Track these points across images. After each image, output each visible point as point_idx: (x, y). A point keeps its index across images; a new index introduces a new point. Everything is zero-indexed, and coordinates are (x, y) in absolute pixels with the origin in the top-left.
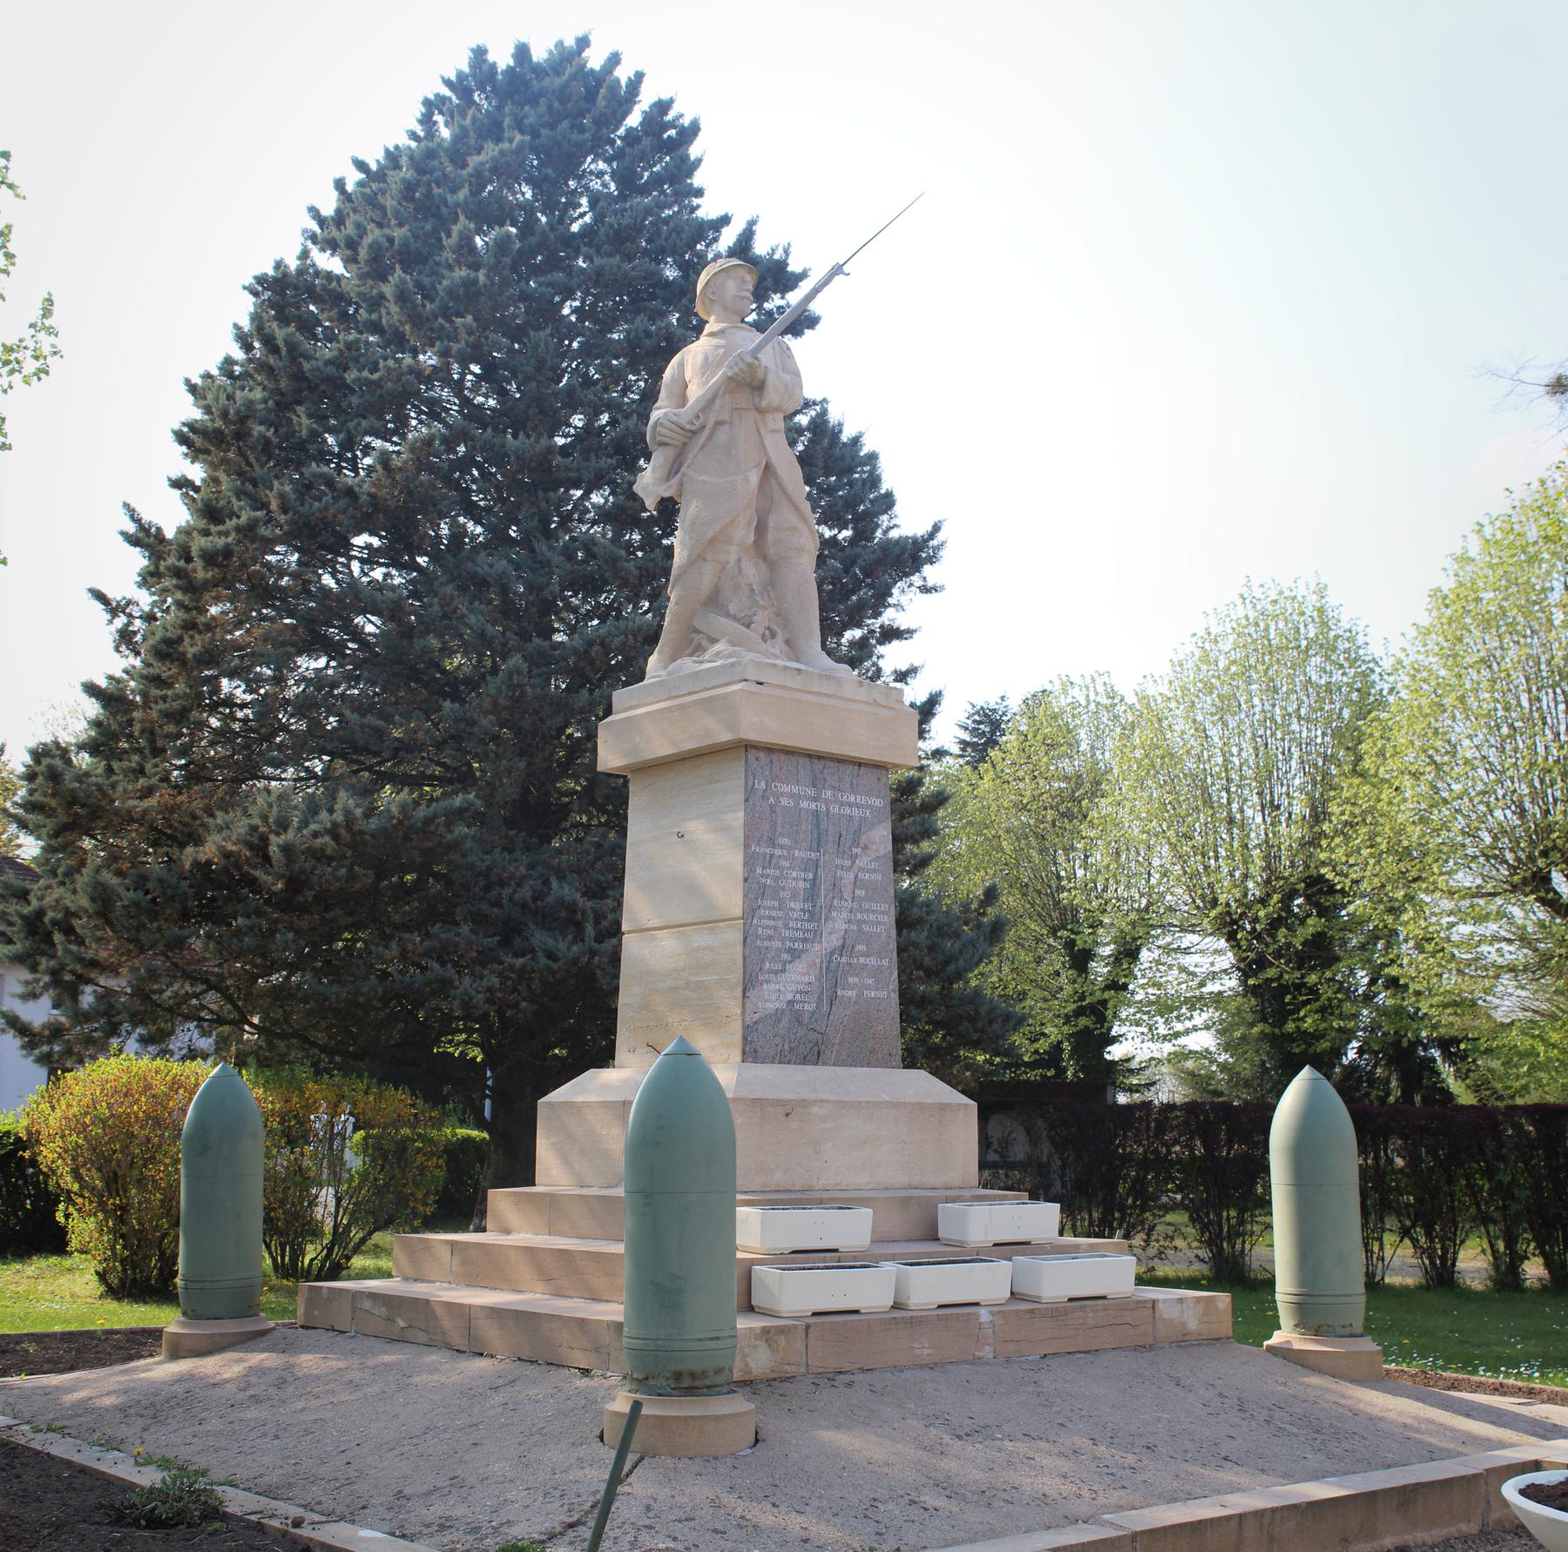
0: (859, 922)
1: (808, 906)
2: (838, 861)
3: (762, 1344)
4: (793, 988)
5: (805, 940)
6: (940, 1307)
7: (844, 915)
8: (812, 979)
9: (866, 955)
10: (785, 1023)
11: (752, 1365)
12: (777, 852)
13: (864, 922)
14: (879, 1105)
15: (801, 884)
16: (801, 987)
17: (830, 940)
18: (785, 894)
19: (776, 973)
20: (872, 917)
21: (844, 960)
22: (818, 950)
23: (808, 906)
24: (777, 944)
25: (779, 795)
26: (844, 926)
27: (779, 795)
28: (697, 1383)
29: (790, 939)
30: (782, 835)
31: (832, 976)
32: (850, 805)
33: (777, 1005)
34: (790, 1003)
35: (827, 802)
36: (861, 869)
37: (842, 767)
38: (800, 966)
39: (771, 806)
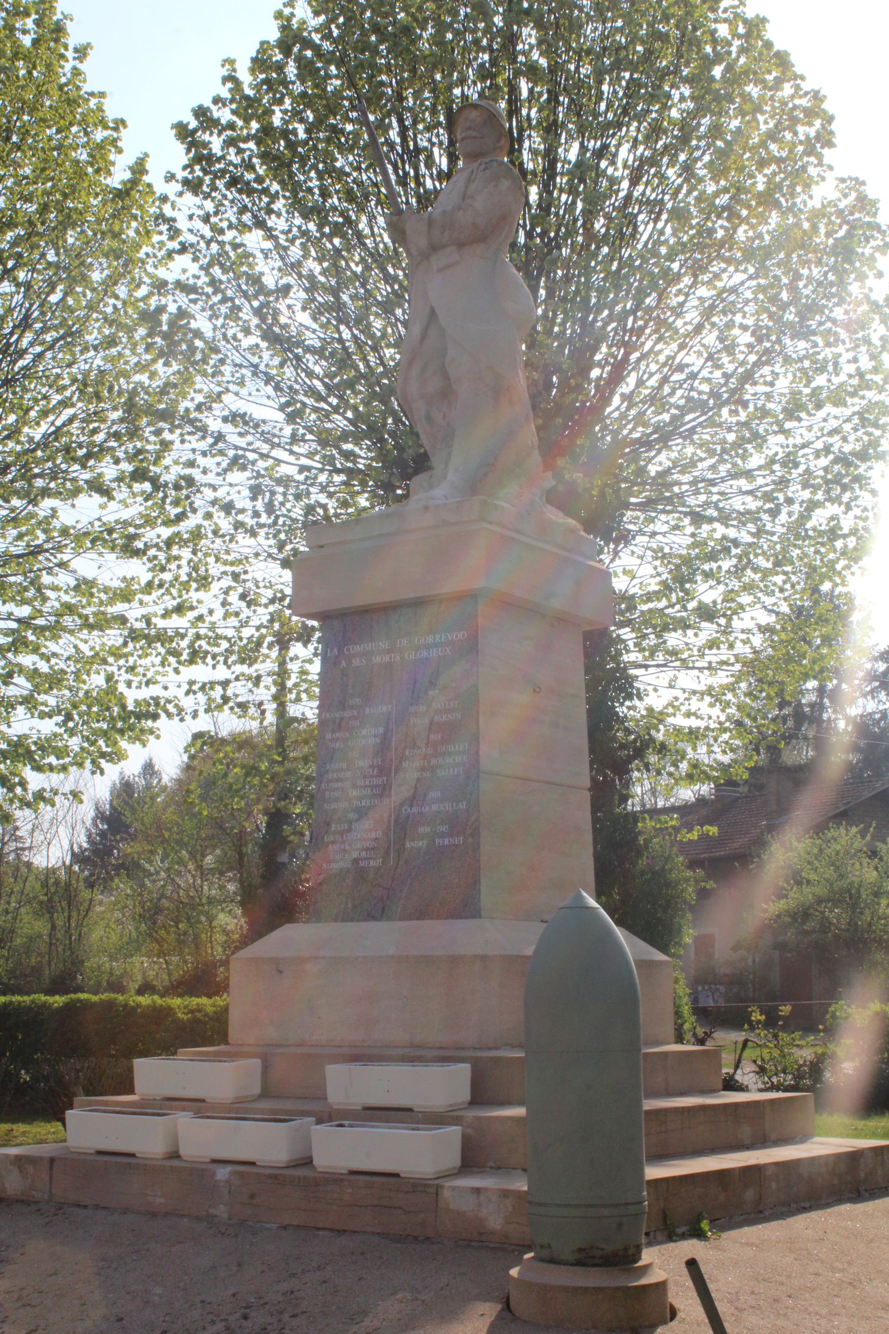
4: (359, 846)
8: (379, 834)
11: (7, 1185)
12: (347, 714)
15: (371, 741)
16: (367, 844)
17: (400, 792)
26: (416, 775)
34: (356, 861)
38: (367, 823)
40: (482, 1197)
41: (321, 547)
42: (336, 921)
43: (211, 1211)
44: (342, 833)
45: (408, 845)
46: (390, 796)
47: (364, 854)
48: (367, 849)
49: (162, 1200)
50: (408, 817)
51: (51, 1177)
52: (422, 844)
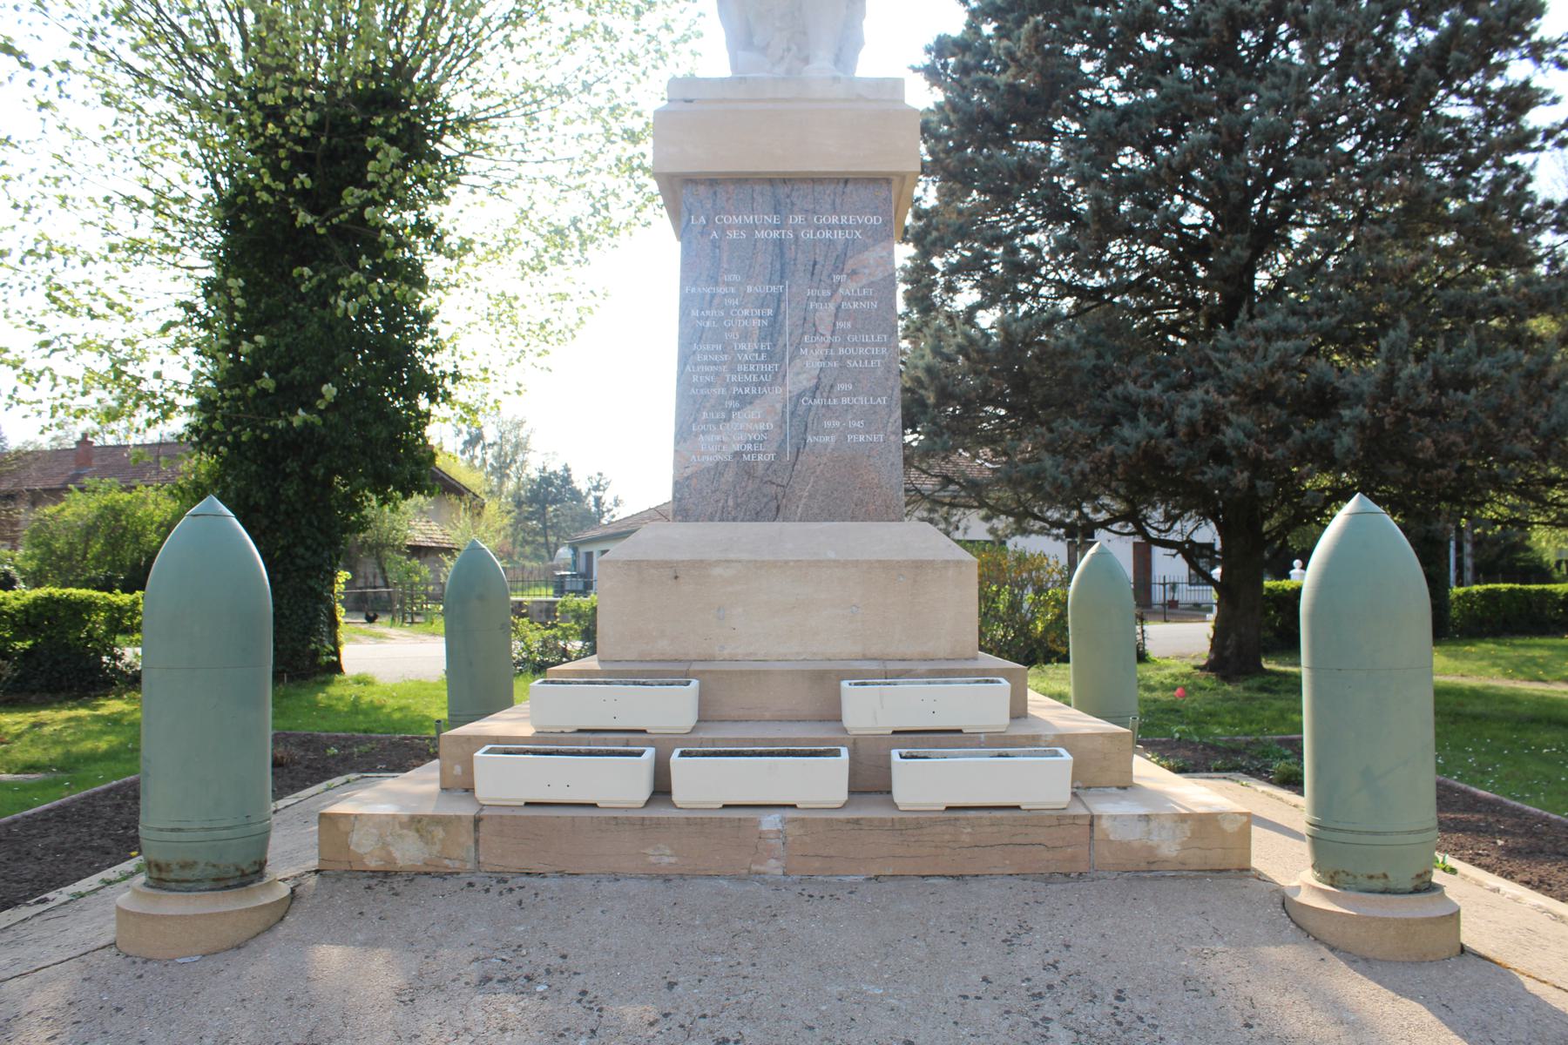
0: (841, 359)
3: (411, 835)
7: (820, 352)
8: (770, 426)
10: (729, 476)
11: (397, 854)
12: (721, 290)
13: (849, 357)
14: (818, 564)
15: (756, 323)
17: (799, 378)
21: (817, 402)
22: (778, 395)
25: (723, 229)
26: (818, 364)
27: (723, 229)
28: (164, 876)
29: (738, 384)
30: (729, 271)
31: (799, 420)
32: (830, 227)
33: (719, 457)
34: (737, 454)
35: (795, 230)
36: (849, 298)
37: (819, 188)
38: (753, 413)
39: (713, 242)
40: (1153, 824)
42: (711, 519)
43: (754, 868)
44: (717, 423)
45: (810, 439)
46: (783, 384)
48: (753, 442)
49: (673, 860)
50: (809, 409)
51: (477, 842)
52: (831, 440)
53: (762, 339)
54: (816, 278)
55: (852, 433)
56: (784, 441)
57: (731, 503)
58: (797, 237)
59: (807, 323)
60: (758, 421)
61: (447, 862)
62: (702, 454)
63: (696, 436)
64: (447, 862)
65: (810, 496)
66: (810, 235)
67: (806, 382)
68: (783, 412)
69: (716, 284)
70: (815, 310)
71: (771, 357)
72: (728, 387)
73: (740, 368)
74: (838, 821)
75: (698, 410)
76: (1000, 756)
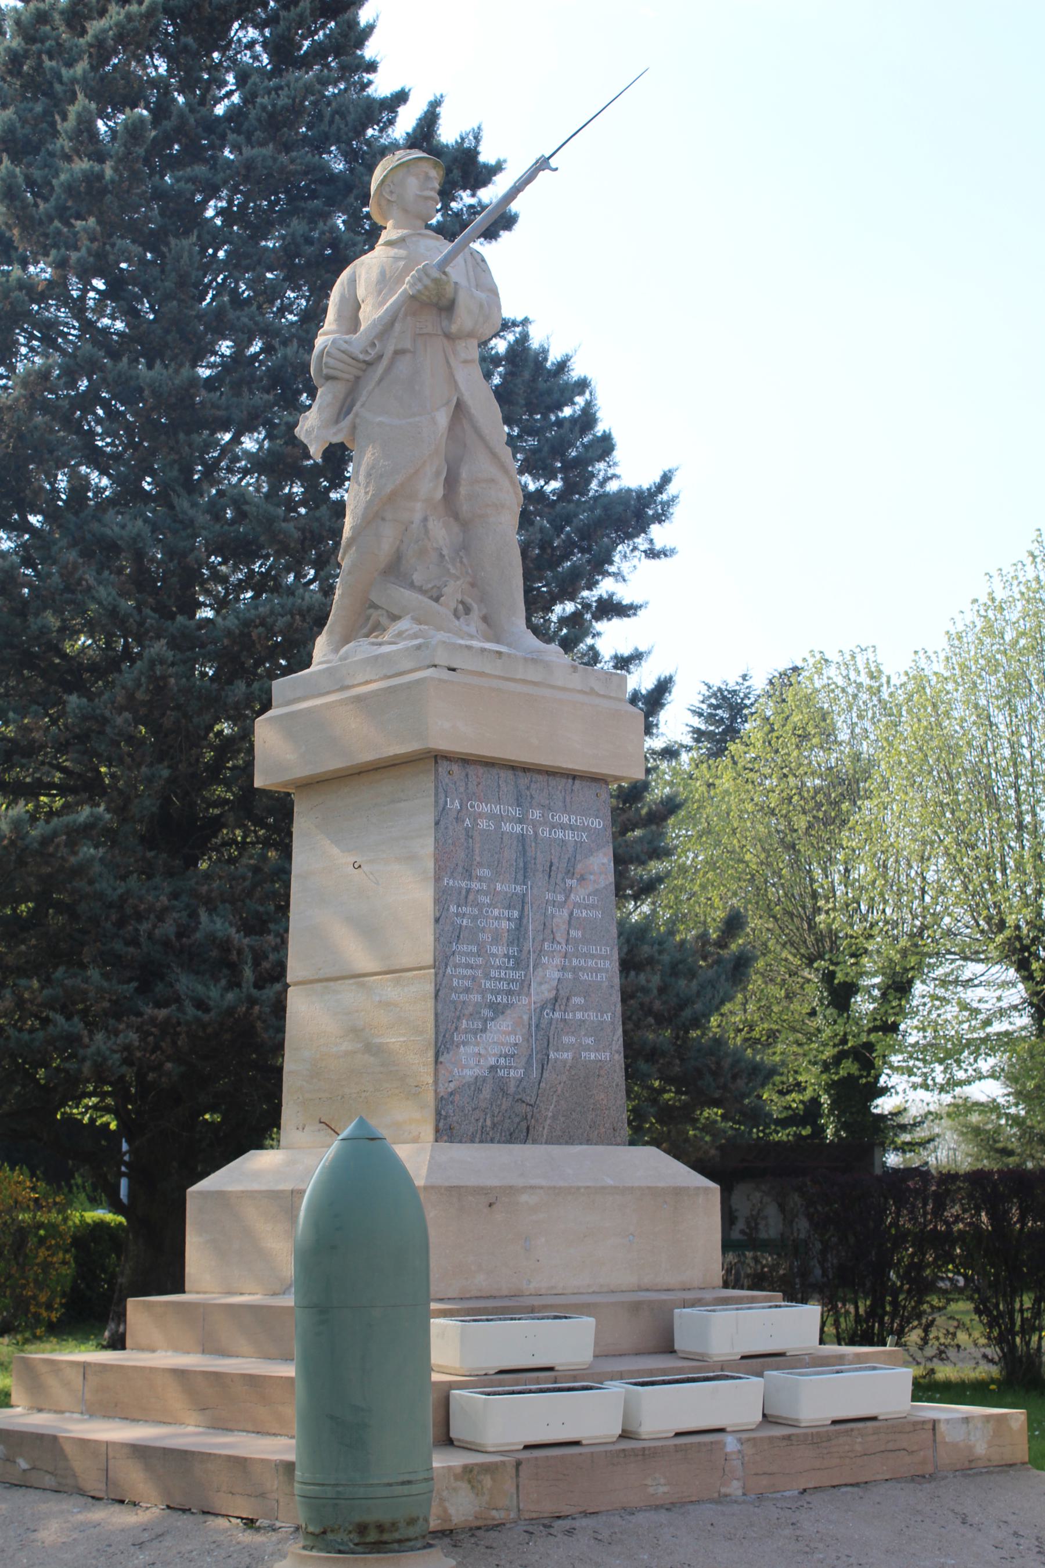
0: (575, 970)
1: (513, 950)
2: (549, 896)
3: (464, 1486)
4: (496, 1051)
5: (509, 993)
6: (678, 1434)
7: (558, 961)
8: (519, 1039)
9: (584, 1008)
10: (486, 1093)
11: (452, 1511)
12: (475, 885)
13: (581, 969)
14: (603, 1190)
15: (505, 924)
16: (506, 1050)
17: (541, 991)
18: (486, 937)
19: (475, 1033)
20: (591, 963)
21: (557, 1015)
23: (513, 950)
24: (476, 998)
25: (476, 817)
26: (557, 975)
27: (476, 817)
28: (386, 1537)
29: (492, 992)
30: (480, 865)
31: (543, 1036)
32: (563, 827)
33: (477, 1071)
34: (493, 1068)
37: (553, 782)
39: (467, 829)
40: (971, 1426)
41: (454, 670)
42: (472, 1141)
43: (723, 1490)
45: (552, 1056)
46: (529, 995)
47: (502, 1061)
49: (665, 1489)
51: (518, 1486)
52: (568, 1056)
53: (510, 944)
54: (552, 880)
55: (585, 1050)
56: (531, 1056)
57: (489, 1123)
58: (536, 833)
59: (546, 926)
60: (509, 1034)
61: (494, 1513)
62: (463, 1067)
63: (458, 1047)
64: (494, 1513)
65: (554, 1118)
66: (546, 834)
67: (546, 992)
68: (530, 1025)
69: (470, 879)
70: (553, 916)
71: (518, 964)
72: (483, 992)
73: (493, 974)
74: (777, 1438)
75: (459, 1018)
76: (838, 1372)
